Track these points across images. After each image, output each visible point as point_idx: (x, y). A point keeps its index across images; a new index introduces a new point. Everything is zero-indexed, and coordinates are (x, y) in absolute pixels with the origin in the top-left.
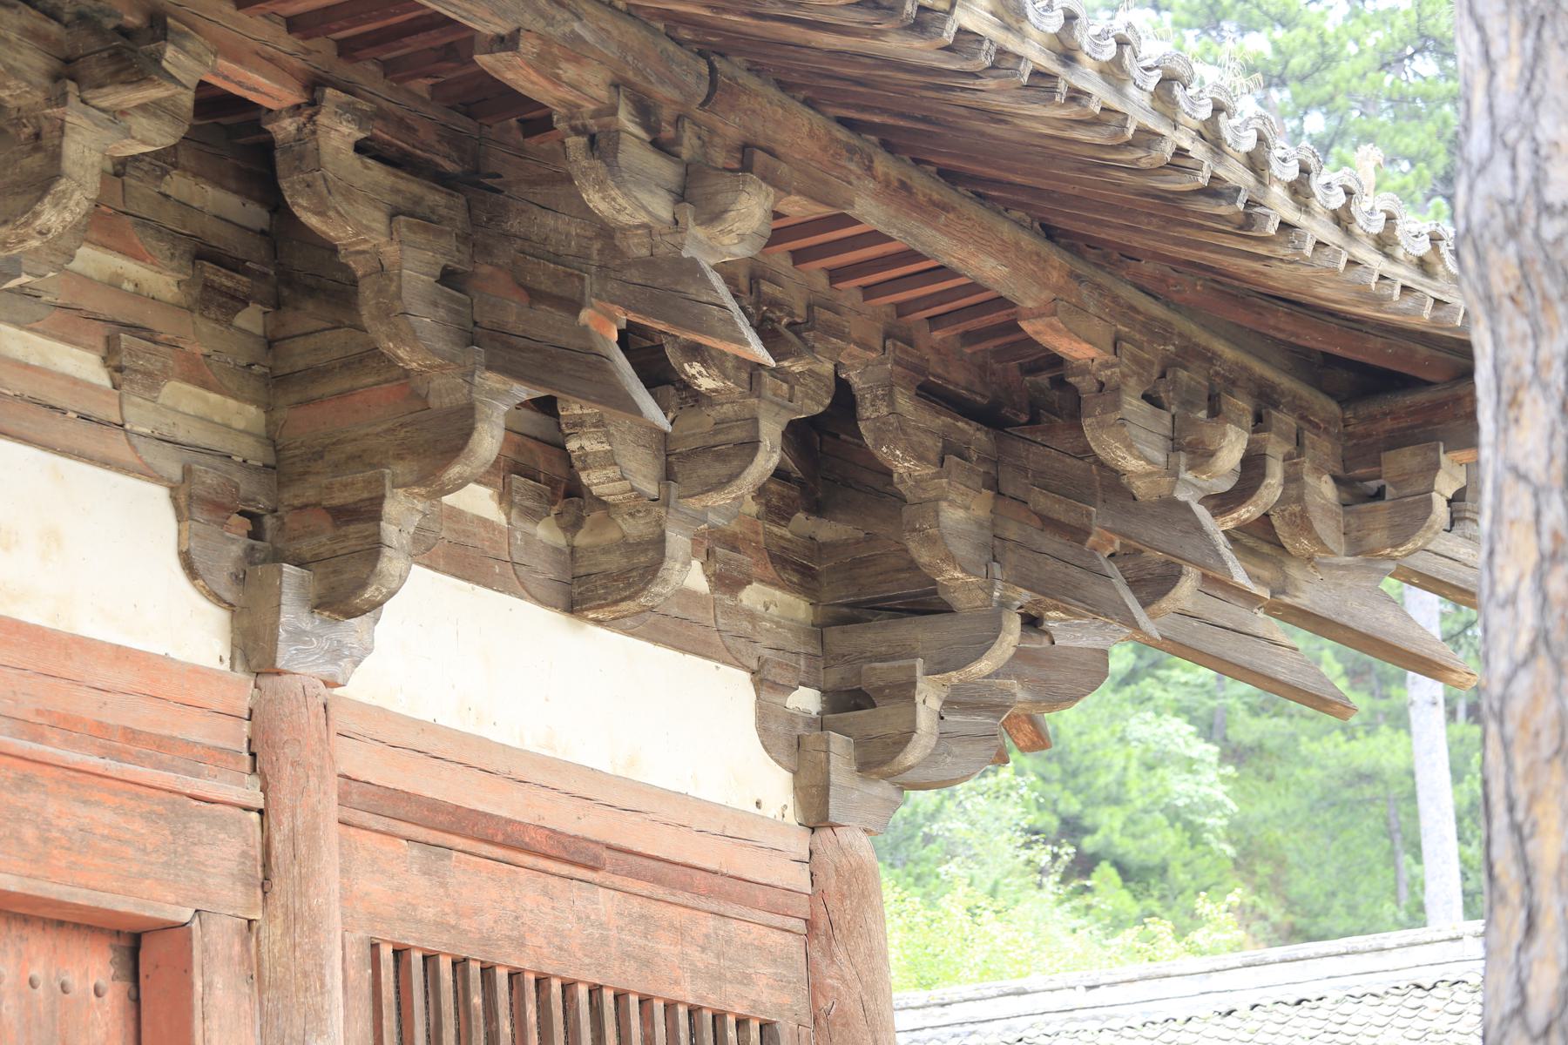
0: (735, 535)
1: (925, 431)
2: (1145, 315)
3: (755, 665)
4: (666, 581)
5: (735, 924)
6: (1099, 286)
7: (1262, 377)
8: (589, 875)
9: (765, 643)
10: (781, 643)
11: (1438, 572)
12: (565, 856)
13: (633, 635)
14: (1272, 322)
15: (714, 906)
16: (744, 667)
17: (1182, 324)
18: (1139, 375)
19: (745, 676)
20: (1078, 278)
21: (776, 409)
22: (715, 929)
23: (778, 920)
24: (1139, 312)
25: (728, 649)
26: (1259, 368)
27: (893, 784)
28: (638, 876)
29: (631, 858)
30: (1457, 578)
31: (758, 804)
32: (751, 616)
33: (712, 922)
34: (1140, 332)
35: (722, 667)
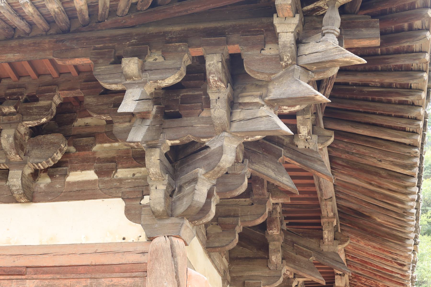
0: (114, 158)
1: (102, 105)
2: (109, 37)
3: (120, 195)
4: (14, 186)
5: (103, 280)
6: (76, 39)
7: (205, 28)
8: (20, 277)
9: (127, 187)
10: (136, 184)
11: (311, 60)
12: (4, 273)
13: (54, 201)
14: (172, 11)
15: (89, 276)
16: (120, 197)
17: (134, 31)
18: (102, 58)
19: (120, 199)
20: (62, 41)
21: (9, 125)
22: (91, 284)
23: (128, 274)
24: (105, 37)
25: (105, 193)
26: (201, 26)
27: (177, 217)
28: (47, 273)
29: (44, 269)
30: (317, 59)
31: (124, 239)
32: (120, 180)
33: (89, 281)
34: (111, 43)
35: (106, 200)
